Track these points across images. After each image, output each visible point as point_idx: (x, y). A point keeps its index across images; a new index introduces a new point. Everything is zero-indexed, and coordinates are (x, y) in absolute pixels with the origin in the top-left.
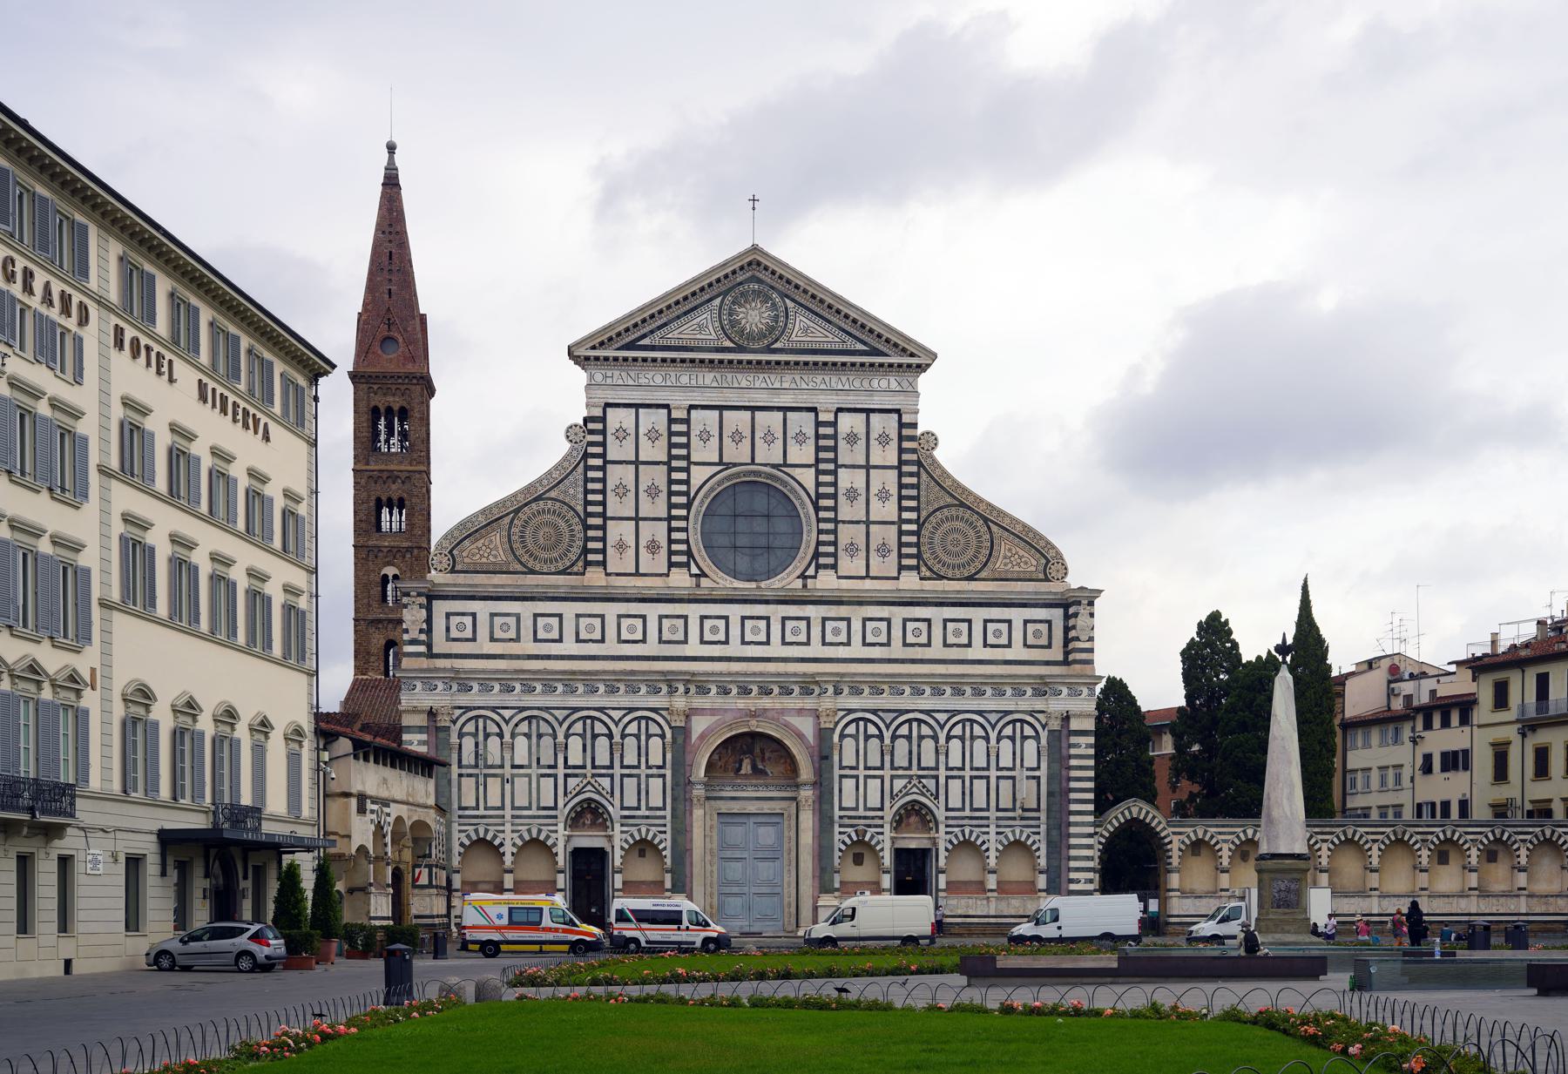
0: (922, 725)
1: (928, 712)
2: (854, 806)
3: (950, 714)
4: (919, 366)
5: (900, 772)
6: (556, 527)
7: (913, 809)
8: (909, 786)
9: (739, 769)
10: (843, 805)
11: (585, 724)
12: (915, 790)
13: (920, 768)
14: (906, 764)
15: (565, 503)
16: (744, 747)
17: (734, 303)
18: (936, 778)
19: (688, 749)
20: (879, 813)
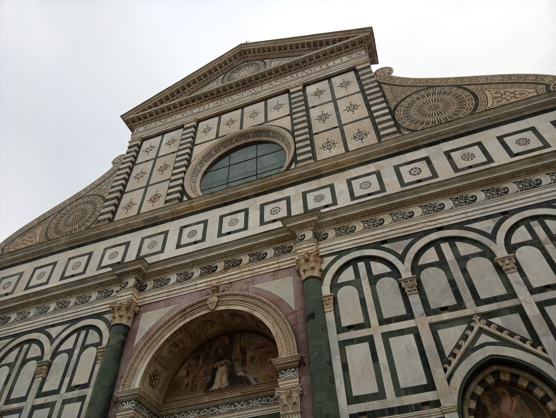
0: (458, 244)
1: (460, 226)
2: (374, 389)
3: (497, 219)
4: (361, 41)
5: (446, 316)
6: (84, 211)
7: (498, 382)
8: (471, 335)
9: (212, 383)
10: (355, 393)
11: (20, 351)
12: (484, 338)
13: (479, 301)
14: (451, 301)
15: (96, 195)
16: (220, 351)
17: (231, 74)
18: (519, 310)
19: (127, 353)
20: (429, 396)
